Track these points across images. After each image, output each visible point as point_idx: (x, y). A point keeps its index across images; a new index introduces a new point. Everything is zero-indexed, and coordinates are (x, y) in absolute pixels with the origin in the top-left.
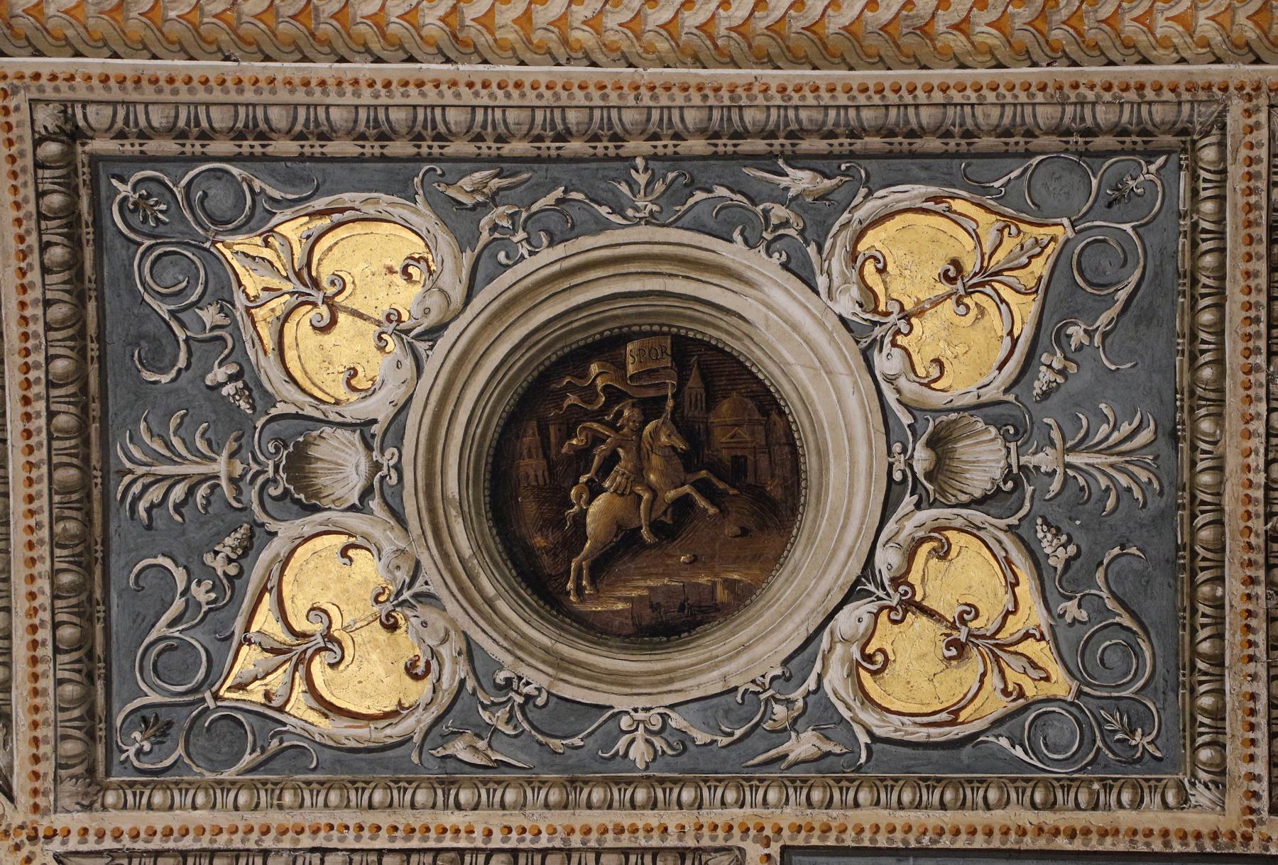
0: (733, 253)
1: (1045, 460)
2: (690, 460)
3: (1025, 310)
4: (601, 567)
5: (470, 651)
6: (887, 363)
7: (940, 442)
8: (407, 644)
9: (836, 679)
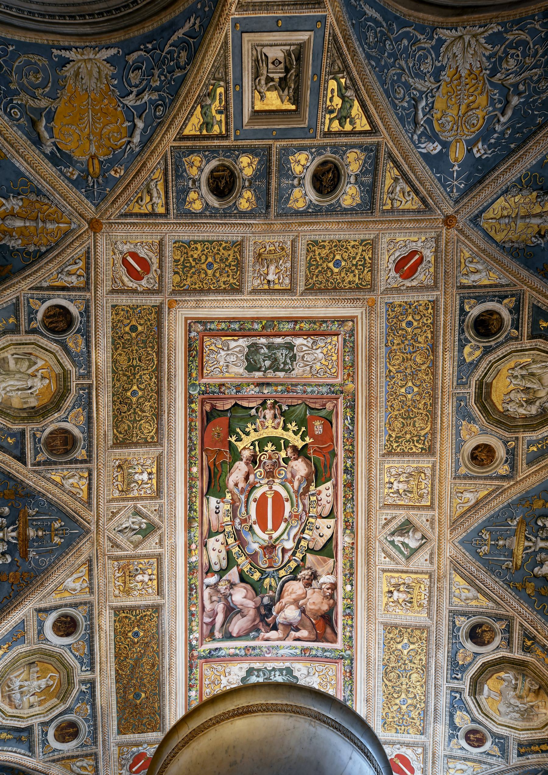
0: (317, 203)
1: (291, 182)
2: (322, 181)
3: (291, 198)
4: (330, 169)
5: (343, 159)
6: (304, 192)
7: (300, 183)
8: (349, 160)
9: (310, 158)
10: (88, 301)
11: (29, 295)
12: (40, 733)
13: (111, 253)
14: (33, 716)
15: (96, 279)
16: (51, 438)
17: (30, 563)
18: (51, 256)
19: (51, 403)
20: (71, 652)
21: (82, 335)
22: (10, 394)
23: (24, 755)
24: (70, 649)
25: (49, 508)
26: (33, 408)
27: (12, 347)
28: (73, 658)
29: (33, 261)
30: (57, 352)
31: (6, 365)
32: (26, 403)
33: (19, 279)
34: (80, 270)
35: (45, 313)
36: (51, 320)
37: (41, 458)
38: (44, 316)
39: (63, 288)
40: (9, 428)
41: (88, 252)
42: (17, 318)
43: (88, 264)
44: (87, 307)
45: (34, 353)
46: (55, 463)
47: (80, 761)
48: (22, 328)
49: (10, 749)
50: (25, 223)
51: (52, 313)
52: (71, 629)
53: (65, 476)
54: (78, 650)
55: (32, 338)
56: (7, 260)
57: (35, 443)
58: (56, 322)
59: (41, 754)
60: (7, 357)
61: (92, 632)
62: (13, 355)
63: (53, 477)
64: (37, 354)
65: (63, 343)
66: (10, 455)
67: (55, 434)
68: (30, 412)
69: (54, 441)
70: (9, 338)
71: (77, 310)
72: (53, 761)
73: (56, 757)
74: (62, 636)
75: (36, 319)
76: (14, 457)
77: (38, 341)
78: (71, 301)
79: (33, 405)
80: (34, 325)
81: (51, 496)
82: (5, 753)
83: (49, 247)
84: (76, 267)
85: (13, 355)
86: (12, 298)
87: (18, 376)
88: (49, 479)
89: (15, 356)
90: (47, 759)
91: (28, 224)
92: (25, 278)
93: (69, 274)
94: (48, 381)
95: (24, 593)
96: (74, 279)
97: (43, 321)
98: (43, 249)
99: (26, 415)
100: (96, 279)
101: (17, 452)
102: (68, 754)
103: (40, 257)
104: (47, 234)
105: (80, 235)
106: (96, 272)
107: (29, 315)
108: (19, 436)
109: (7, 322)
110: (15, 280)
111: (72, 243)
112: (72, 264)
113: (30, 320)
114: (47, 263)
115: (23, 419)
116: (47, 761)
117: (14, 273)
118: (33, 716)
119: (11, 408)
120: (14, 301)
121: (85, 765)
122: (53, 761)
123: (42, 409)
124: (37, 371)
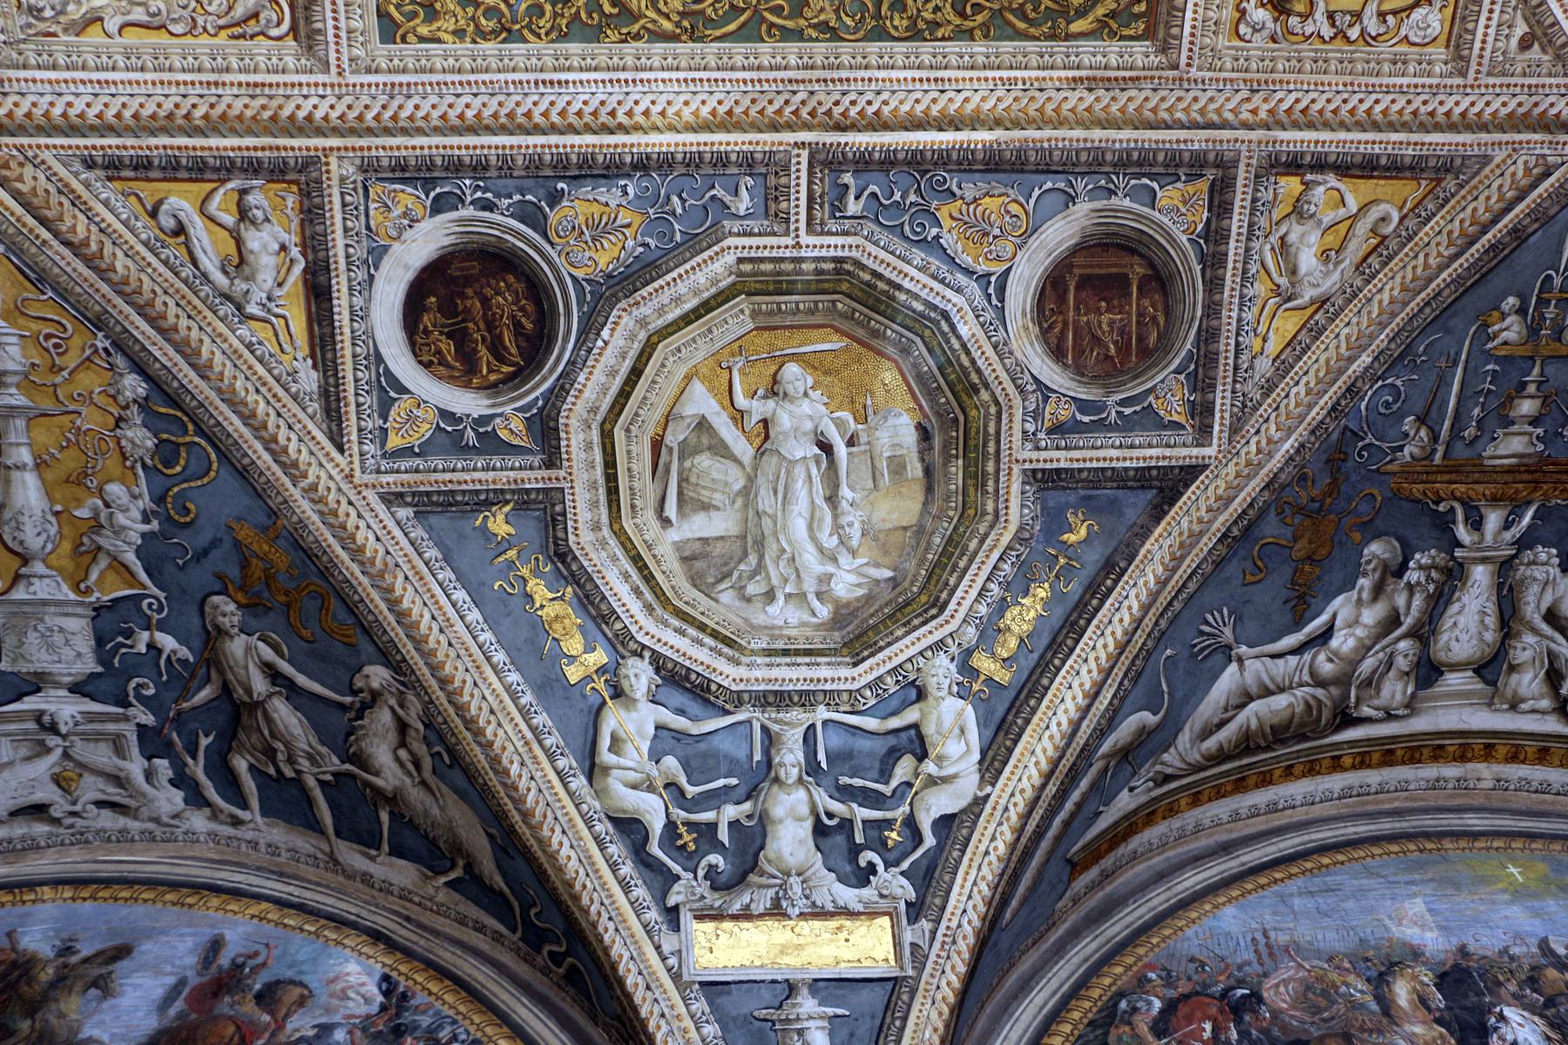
10: (369, 168)
11: (370, 448)
13: (93, 36)
15: (250, 126)
16: (1079, 352)
18: (162, 352)
19: (905, 351)
21: (555, 198)
22: (856, 532)
25: (1415, 367)
26: (924, 433)
27: (628, 525)
29: (200, 431)
30: (643, 323)
31: (718, 549)
32: (897, 466)
33: (296, 493)
34: (213, 207)
35: (451, 379)
36: (483, 352)
37: (1173, 402)
38: (467, 385)
39: (318, 292)
40: (1019, 538)
41: (113, 167)
42: (486, 501)
43: (173, 169)
44: (402, 172)
45: (651, 430)
46: (1208, 335)
48: (535, 479)
50: (21, 467)
51: (448, 347)
53: (1277, 290)
55: (578, 439)
56: (215, 543)
57: (1101, 426)
58: (490, 326)
60: (678, 546)
62: (666, 522)
63: (1273, 347)
64: (658, 414)
65: (597, 297)
66: (1145, 533)
67: (1062, 338)
68: (946, 446)
69: (1097, 341)
70: (586, 536)
71: (426, 225)
75: (484, 420)
76: (1158, 520)
77: (593, 410)
78: (377, 254)
79: (910, 437)
80: (512, 428)
81: (1365, 359)
83: (119, 361)
84: (198, 229)
85: (666, 522)
86: (391, 524)
87: (766, 501)
88: (1283, 367)
89: (671, 510)
91: (25, 455)
92: (292, 469)
93: (240, 263)
94: (792, 370)
96: (260, 241)
97: (491, 388)
98: (133, 385)
99: (957, 469)
100: (250, 126)
101: (1136, 504)
103: (174, 402)
104: (55, 369)
105: (27, 206)
106: (213, 126)
107: (466, 450)
108: (1055, 498)
109: (506, 544)
110: (305, 507)
111: (77, 248)
112: (187, 245)
113: (491, 444)
114: (203, 371)
115: (976, 478)
117: (273, 514)
119: (920, 531)
120: (404, 513)
123: (931, 395)
124: (739, 416)
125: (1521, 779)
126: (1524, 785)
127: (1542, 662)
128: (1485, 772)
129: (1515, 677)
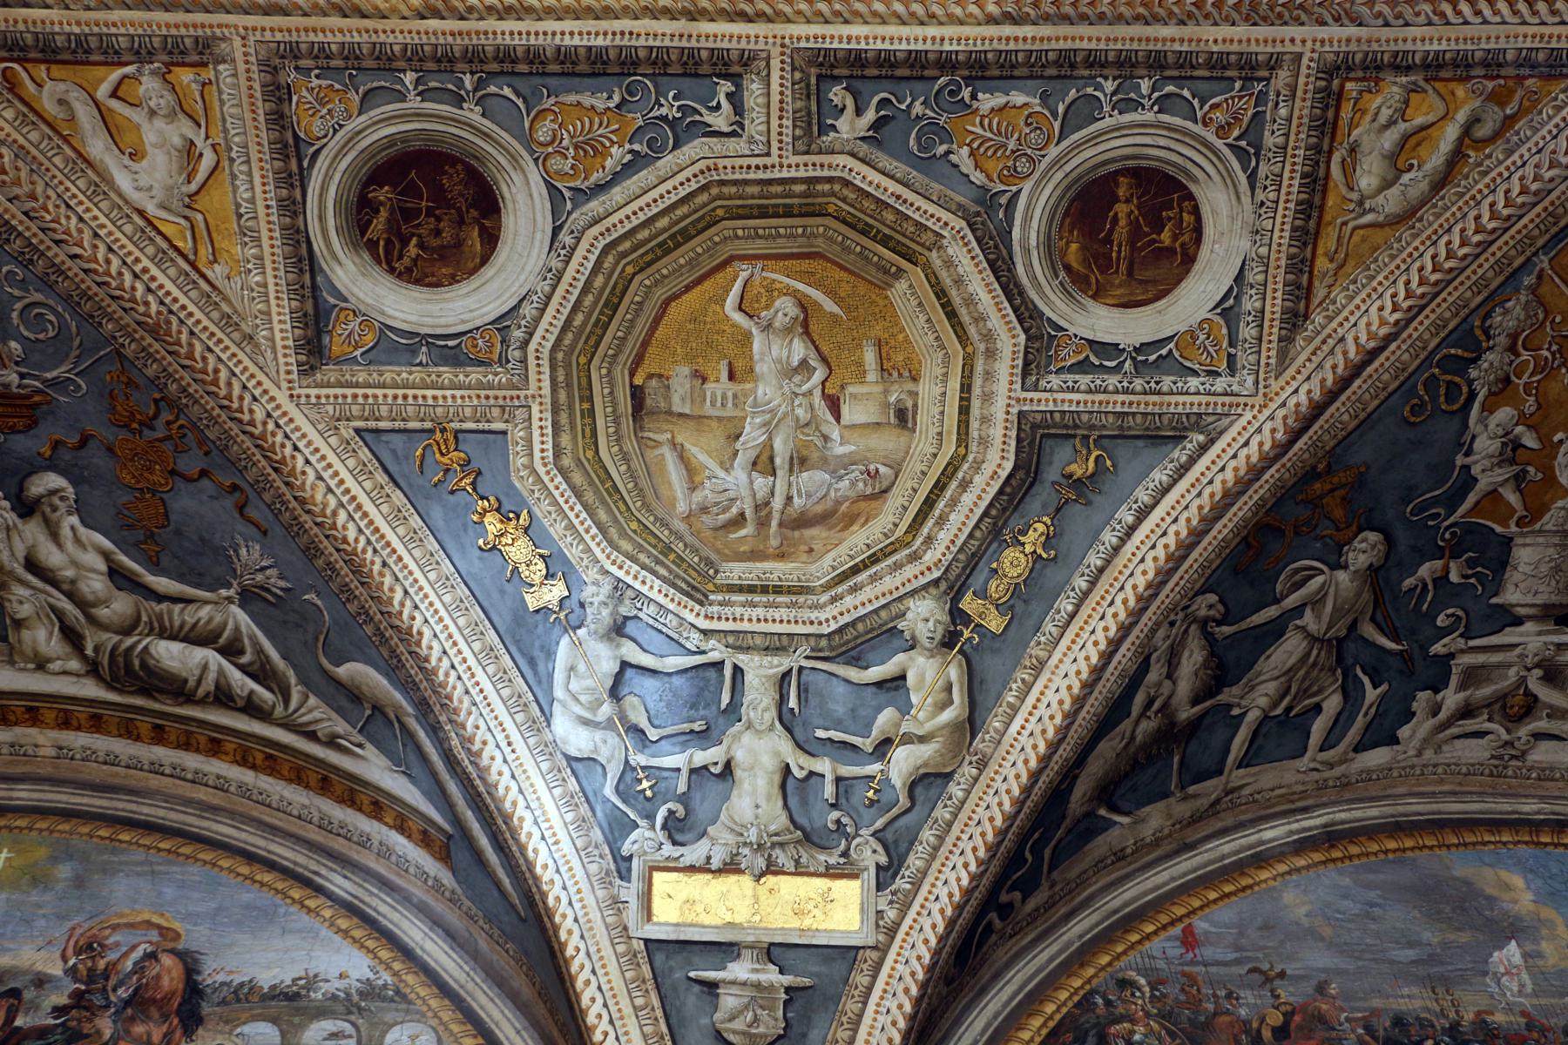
12: (1084, 380)
14: (964, 410)
17: (55, 383)
20: (601, 188)
23: (1183, 470)
24: (583, 195)
28: (644, 177)
47: (1349, 169)
49: (1109, 537)
52: (452, 182)
54: (591, 149)
59: (1220, 384)
61: (474, 57)
72: (1295, 319)
73: (1275, 304)
74: (491, 239)
82: (1120, 561)
90: (1270, 353)
95: (214, 421)
102: (1282, 237)
116: (1284, 358)
118: (964, 410)
121: (1389, 139)
122: (1295, 319)
125: (85, 749)
126: (89, 756)
127: (48, 616)
128: (44, 740)
129: (26, 634)
